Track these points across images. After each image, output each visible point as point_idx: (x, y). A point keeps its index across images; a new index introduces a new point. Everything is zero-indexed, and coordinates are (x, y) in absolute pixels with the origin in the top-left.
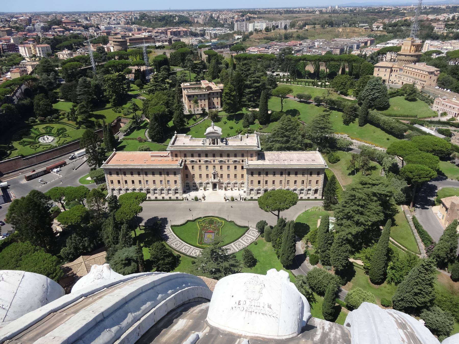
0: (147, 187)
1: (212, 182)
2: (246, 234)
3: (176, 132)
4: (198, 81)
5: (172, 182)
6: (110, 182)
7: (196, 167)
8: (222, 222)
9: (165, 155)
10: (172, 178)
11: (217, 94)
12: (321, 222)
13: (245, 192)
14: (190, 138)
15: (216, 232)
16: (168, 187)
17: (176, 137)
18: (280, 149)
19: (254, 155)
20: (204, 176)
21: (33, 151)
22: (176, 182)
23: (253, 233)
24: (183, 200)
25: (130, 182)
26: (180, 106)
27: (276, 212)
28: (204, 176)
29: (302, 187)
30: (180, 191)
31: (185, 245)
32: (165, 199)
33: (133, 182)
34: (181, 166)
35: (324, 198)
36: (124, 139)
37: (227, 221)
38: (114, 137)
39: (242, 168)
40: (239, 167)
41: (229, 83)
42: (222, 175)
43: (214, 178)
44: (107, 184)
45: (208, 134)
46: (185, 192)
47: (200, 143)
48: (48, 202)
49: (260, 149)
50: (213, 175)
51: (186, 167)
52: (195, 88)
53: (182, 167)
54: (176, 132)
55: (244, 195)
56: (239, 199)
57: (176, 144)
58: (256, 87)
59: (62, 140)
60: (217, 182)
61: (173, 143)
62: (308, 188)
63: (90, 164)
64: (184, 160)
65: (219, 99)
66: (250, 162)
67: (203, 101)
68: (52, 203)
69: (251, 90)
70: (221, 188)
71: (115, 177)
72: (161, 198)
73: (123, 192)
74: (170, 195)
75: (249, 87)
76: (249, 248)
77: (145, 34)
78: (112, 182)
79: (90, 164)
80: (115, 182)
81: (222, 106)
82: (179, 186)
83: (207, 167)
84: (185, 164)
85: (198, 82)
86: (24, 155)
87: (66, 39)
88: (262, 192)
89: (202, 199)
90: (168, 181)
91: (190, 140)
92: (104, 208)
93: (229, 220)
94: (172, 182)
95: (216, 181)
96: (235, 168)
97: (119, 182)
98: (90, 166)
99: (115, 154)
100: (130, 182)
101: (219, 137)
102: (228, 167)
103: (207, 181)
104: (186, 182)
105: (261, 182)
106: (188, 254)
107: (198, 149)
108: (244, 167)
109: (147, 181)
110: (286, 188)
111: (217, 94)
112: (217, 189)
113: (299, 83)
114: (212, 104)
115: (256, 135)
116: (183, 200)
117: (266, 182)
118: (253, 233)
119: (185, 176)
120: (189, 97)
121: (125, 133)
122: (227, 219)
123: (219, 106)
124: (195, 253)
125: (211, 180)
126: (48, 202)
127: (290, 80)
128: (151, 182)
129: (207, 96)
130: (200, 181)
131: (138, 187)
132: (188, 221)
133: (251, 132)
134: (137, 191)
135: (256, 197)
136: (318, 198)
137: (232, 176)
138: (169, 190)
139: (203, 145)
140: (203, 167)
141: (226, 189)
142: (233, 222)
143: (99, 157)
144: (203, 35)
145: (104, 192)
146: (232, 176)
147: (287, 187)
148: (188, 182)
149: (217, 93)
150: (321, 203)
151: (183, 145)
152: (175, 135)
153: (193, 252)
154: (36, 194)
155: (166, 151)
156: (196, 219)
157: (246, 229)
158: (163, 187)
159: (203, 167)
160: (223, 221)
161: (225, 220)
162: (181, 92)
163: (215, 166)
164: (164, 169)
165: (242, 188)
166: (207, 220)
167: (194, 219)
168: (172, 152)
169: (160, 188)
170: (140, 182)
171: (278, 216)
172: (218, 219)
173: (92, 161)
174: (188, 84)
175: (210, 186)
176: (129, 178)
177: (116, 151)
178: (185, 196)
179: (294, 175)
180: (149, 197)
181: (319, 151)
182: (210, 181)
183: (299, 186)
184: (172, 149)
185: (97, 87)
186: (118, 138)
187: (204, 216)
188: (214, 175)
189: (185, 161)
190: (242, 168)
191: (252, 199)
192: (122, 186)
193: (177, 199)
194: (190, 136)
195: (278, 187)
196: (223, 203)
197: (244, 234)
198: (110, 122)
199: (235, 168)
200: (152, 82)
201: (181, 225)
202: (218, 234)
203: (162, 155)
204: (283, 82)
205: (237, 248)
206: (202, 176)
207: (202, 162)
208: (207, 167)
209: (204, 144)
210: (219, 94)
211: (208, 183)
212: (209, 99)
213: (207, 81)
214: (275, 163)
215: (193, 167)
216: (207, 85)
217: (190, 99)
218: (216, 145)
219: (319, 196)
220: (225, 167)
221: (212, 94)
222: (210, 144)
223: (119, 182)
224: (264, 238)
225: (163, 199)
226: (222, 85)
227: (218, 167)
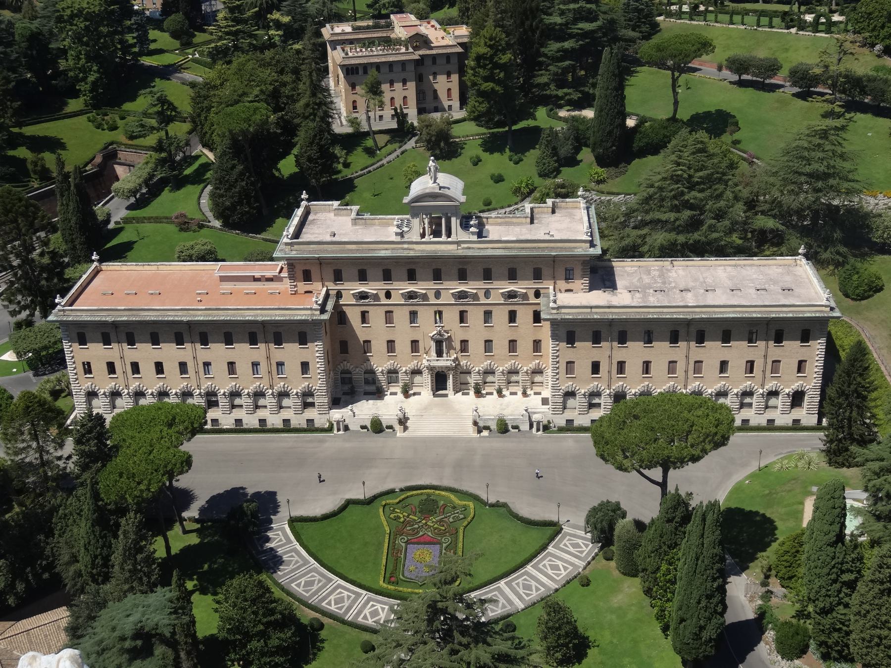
0: (206, 385)
1: (431, 369)
2: (550, 549)
3: (304, 196)
4: (381, 17)
5: (293, 368)
6: (80, 369)
7: (376, 315)
8: (465, 508)
9: (269, 274)
11: (448, 61)
12: (816, 508)
13: (545, 401)
14: (353, 215)
15: (446, 541)
17: (307, 213)
18: (670, 251)
19: (578, 271)
20: (404, 346)
23: (576, 546)
24: (330, 429)
25: (148, 369)
26: (320, 104)
27: (656, 473)
28: (404, 346)
29: (747, 384)
30: (321, 399)
31: (339, 586)
32: (269, 426)
33: (159, 368)
34: (323, 310)
35: (825, 422)
36: (127, 220)
37: (485, 503)
38: (93, 215)
39: (537, 318)
40: (525, 315)
41: (490, 23)
42: (464, 343)
43: (439, 353)
44: (72, 377)
45: (419, 198)
46: (336, 402)
47: (390, 233)
49: (598, 251)
50: (433, 345)
51: (340, 316)
52: (369, 43)
53: (326, 317)
54: (304, 196)
55: (543, 413)
56: (525, 427)
57: (305, 237)
58: (585, 34)
60: (448, 368)
61: (297, 234)
62: (770, 385)
63: (12, 307)
64: (333, 293)
65: (455, 78)
66: (564, 299)
67: (398, 86)
69: (567, 45)
70: (462, 387)
72: (256, 424)
73: (124, 404)
74: (286, 414)
75: (560, 34)
76: (560, 598)
78: (88, 368)
79: (12, 307)
80: (99, 368)
81: (463, 102)
82: (318, 381)
83: (413, 315)
84: (337, 306)
85: (382, 22)
88: (605, 401)
89: (398, 427)
90: (280, 364)
91: (355, 222)
92: (59, 458)
93: (492, 500)
94: (293, 368)
95: (445, 362)
96: (512, 316)
97: (111, 368)
98: (13, 313)
99: (97, 272)
100: (148, 369)
101: (455, 210)
102: (488, 315)
103: (412, 365)
104: (341, 367)
105: (604, 368)
106: (349, 617)
107: (383, 253)
108: (543, 316)
109: (207, 365)
110: (690, 389)
111: (448, 61)
112: (450, 391)
113: (737, 18)
114: (429, 96)
115: (582, 204)
116: (330, 429)
117: (621, 367)
118: (576, 546)
119: (338, 346)
121: (132, 200)
122: (484, 496)
123: (456, 104)
124: (375, 613)
125: (429, 359)
127: (702, 8)
128: (219, 369)
130: (388, 365)
131: (175, 384)
132: (349, 503)
133: (566, 192)
134: (172, 400)
135: (583, 420)
136: (804, 422)
137: (500, 346)
138: (284, 394)
139: (398, 239)
141: (478, 393)
142: (505, 505)
143: (43, 282)
145: (61, 403)
146: (500, 346)
147: (694, 385)
148: (349, 366)
149: (448, 56)
150: (815, 442)
151: (328, 238)
152: (304, 203)
153: (367, 611)
155: (272, 259)
156: (375, 498)
157: (550, 531)
158: (264, 385)
159: (401, 316)
160: (471, 505)
161: (476, 498)
162: (324, 57)
163: (440, 313)
164: (264, 324)
165: (537, 389)
167: (369, 494)
168: (292, 264)
169: (251, 389)
170: (183, 367)
171: (663, 485)
172: (452, 497)
173: (19, 298)
174: (347, 28)
175: (424, 384)
176: (145, 353)
177: (101, 261)
178: (336, 414)
179: (641, 344)
180: (215, 421)
181: (807, 256)
182: (425, 362)
183: (737, 383)
184: (293, 254)
185: (37, 40)
186: (109, 216)
187: (403, 485)
188: (439, 343)
189: (339, 295)
190: (537, 318)
191: (570, 427)
193: (310, 427)
194: (355, 208)
195: (660, 385)
196: (470, 440)
197: (544, 547)
198: (80, 163)
199: (512, 316)
200: (223, 23)
201: (325, 517)
202: (452, 546)
203: (257, 275)
204: (679, 14)
205: (520, 598)
206: (397, 346)
207: (396, 299)
208: (413, 315)
209: (402, 235)
210: (454, 60)
211: (417, 372)
212: (420, 79)
213: (412, 17)
214: (653, 300)
215: (364, 316)
216: (413, 32)
217: (354, 78)
218: (444, 238)
219: (807, 414)
221: (428, 62)
223: (111, 368)
224: (613, 564)
225: (263, 428)
226: (463, 31)
227: (451, 316)
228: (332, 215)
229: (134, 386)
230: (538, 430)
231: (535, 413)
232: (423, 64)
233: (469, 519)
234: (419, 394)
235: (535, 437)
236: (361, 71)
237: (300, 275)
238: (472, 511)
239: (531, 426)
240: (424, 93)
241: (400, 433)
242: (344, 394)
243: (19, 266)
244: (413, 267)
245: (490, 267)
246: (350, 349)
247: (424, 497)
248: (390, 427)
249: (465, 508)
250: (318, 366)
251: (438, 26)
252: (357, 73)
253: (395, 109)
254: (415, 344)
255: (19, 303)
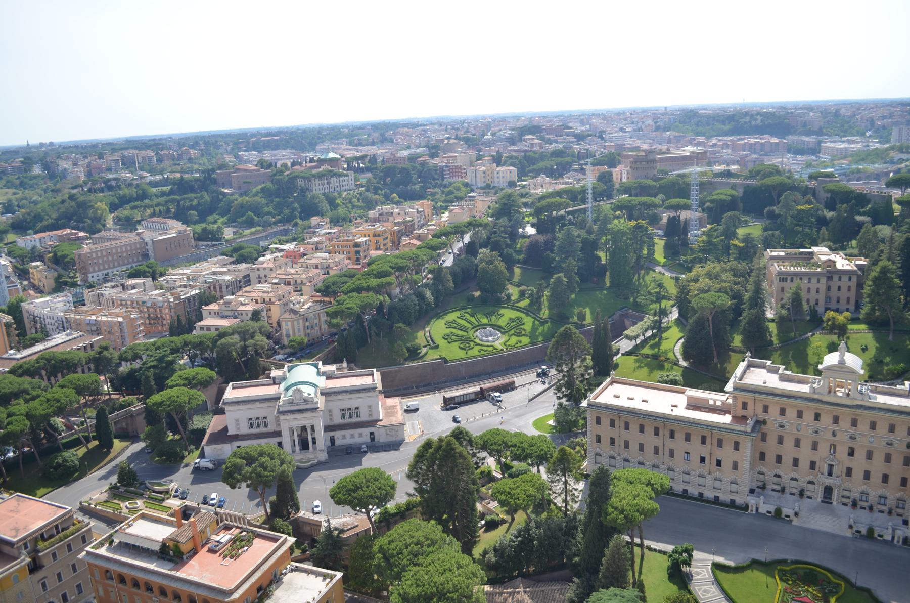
8: (838, 585)
10: (727, 454)
16: (718, 474)
21: (461, 354)
22: (735, 466)
24: (746, 508)
33: (641, 448)
38: (610, 347)
43: (830, 474)
45: (829, 368)
48: (478, 455)
56: (888, 537)
59: (514, 340)
61: (741, 379)
63: (559, 394)
68: (484, 458)
71: (605, 431)
77: (688, 150)
79: (559, 394)
86: (448, 358)
87: (542, 156)
92: (576, 490)
93: (860, 583)
94: (727, 464)
97: (613, 441)
98: (559, 398)
103: (810, 478)
104: (759, 469)
119: (758, 455)
120: (783, 277)
122: (853, 580)
126: (478, 455)
129: (823, 280)
140: (806, 445)
142: (868, 591)
143: (578, 383)
144: (815, 150)
148: (764, 470)
154: (459, 435)
155: (724, 392)
160: (843, 584)
163: (835, 446)
165: (900, 511)
166: (802, 572)
169: (698, 472)
170: (656, 450)
172: (829, 575)
173: (564, 389)
178: (752, 501)
186: (619, 350)
187: (794, 558)
188: (831, 466)
192: (617, 450)
199: (888, 459)
210: (854, 279)
213: (826, 250)
220: (860, 454)
222: (830, 392)
223: (613, 441)
228: (765, 371)
229: (625, 455)
230: (898, 542)
231: (897, 529)
232: (832, 279)
233: (840, 594)
234: (811, 498)
235: (895, 546)
236: (789, 280)
237: (740, 405)
238: (843, 589)
239: (893, 538)
240: (830, 298)
241: (796, 522)
242: (758, 487)
243: (567, 371)
244: (818, 411)
245: (876, 420)
246: (766, 458)
247: (808, 571)
248: (788, 516)
249: (838, 585)
250: (745, 465)
251: (844, 257)
252: (786, 281)
253: (811, 306)
254: (813, 465)
255: (563, 392)
